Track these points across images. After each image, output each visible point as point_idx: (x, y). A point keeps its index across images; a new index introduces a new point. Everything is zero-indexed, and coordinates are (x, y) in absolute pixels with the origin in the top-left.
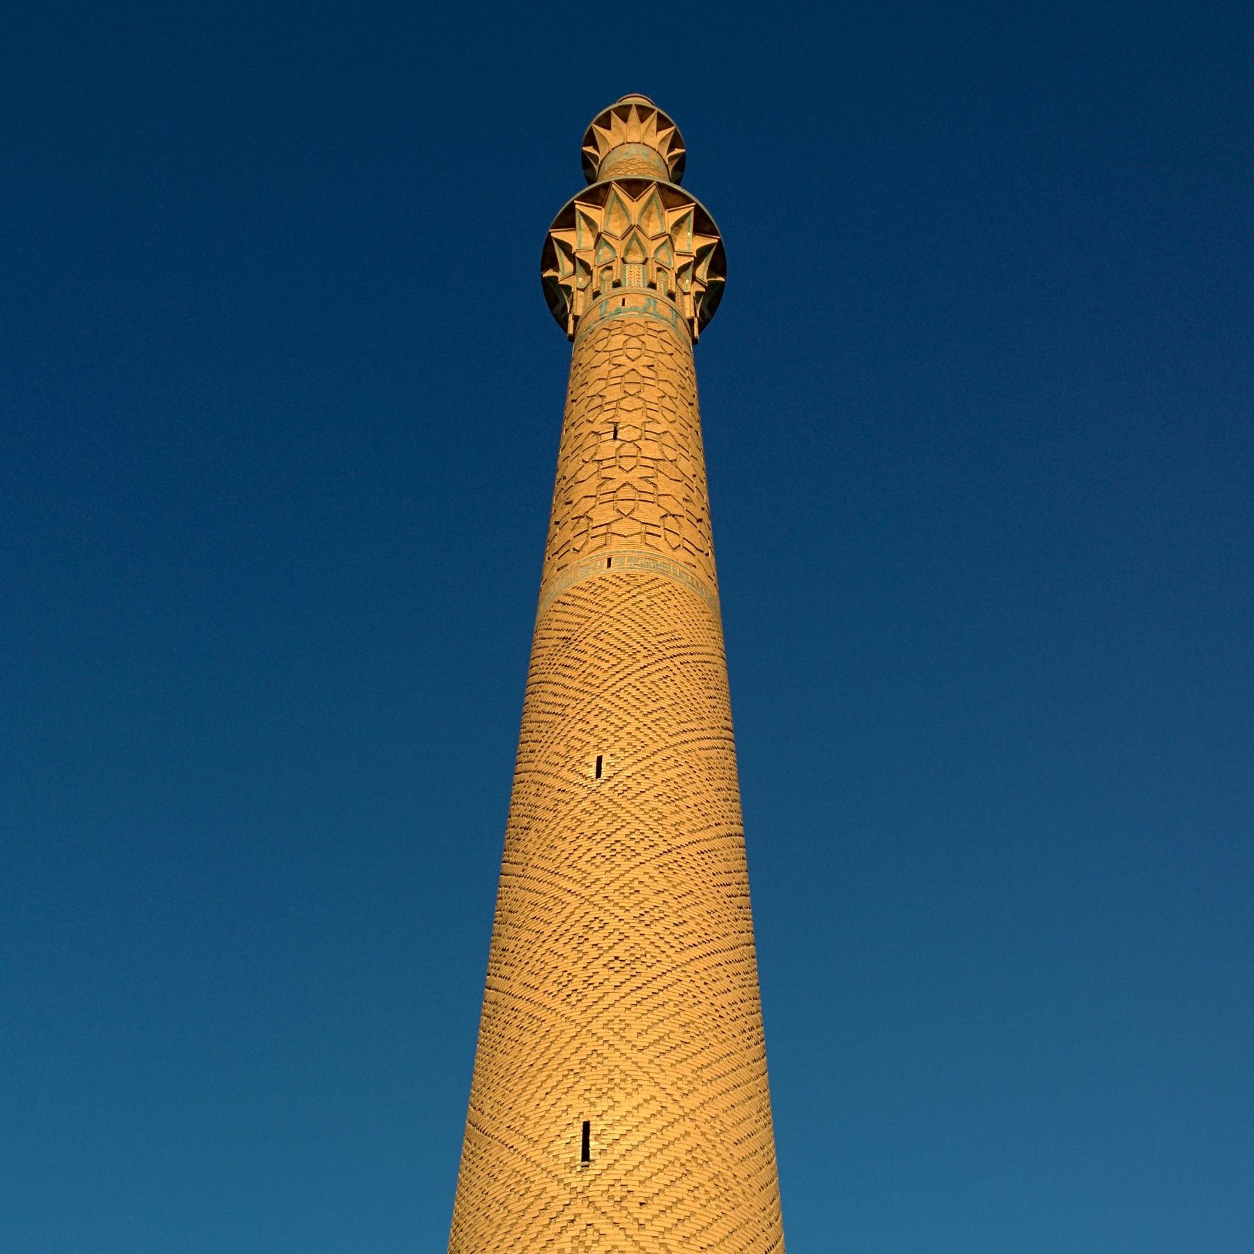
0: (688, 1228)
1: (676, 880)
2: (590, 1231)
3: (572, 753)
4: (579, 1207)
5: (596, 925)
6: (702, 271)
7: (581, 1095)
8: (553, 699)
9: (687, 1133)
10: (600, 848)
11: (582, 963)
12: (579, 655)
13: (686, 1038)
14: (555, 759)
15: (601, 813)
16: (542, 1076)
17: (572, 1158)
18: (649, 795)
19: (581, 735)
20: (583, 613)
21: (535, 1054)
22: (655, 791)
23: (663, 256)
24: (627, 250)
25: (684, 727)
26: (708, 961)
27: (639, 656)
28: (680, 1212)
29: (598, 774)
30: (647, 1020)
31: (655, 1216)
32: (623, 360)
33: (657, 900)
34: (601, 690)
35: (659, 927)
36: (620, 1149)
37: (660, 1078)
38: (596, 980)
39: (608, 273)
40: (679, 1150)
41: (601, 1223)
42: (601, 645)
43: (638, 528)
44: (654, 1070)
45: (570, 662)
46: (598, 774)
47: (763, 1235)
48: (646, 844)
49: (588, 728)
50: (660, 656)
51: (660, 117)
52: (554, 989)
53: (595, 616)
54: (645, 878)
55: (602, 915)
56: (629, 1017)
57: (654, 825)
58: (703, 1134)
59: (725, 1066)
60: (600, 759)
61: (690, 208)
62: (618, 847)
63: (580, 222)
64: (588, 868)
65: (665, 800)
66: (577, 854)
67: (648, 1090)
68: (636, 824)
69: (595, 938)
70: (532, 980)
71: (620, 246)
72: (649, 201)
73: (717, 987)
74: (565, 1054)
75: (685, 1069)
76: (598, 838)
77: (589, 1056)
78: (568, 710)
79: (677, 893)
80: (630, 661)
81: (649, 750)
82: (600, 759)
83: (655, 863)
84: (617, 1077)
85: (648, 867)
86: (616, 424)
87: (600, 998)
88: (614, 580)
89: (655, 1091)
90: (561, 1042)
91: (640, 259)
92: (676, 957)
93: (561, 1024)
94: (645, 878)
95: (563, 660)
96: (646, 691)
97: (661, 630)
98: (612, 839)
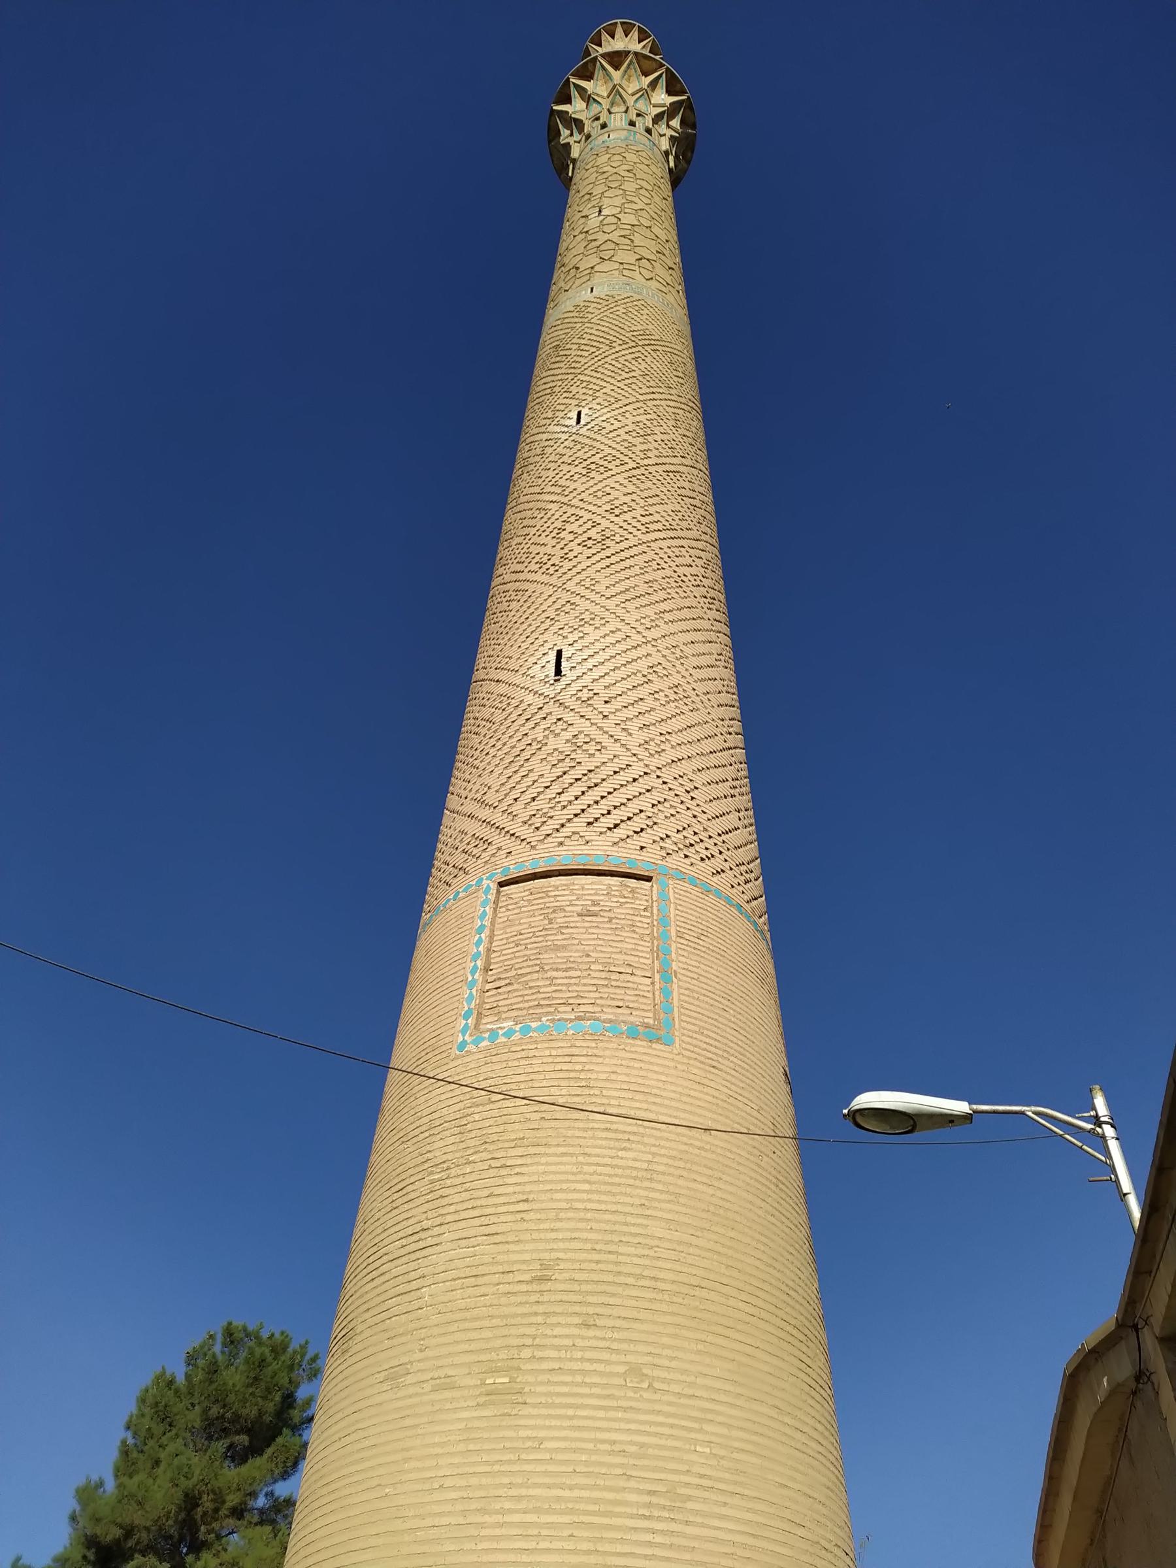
0: (648, 719)
1: (643, 487)
2: (560, 723)
5: (573, 519)
6: (676, 123)
10: (579, 469)
11: (559, 546)
13: (650, 591)
14: (544, 422)
15: (579, 446)
17: (547, 676)
18: (621, 432)
19: (565, 401)
22: (627, 429)
23: (642, 105)
24: (612, 104)
25: (652, 390)
28: (641, 707)
29: (578, 422)
30: (614, 578)
32: (608, 168)
33: (628, 499)
35: (628, 516)
37: (626, 617)
38: (571, 555)
40: (642, 665)
41: (569, 717)
43: (617, 266)
46: (578, 422)
47: (730, 783)
48: (618, 462)
51: (640, 30)
54: (617, 486)
55: (577, 512)
56: (598, 576)
57: (625, 451)
58: (664, 656)
59: (686, 613)
60: (579, 413)
61: (663, 70)
62: (593, 466)
65: (634, 434)
67: (614, 624)
68: (608, 451)
69: (569, 528)
70: (519, 567)
71: (606, 103)
72: (629, 65)
73: (679, 561)
74: (543, 607)
75: (649, 611)
81: (620, 404)
82: (579, 413)
83: (626, 475)
84: (587, 616)
85: (619, 478)
89: (620, 625)
90: (540, 600)
94: (617, 486)
97: (634, 328)
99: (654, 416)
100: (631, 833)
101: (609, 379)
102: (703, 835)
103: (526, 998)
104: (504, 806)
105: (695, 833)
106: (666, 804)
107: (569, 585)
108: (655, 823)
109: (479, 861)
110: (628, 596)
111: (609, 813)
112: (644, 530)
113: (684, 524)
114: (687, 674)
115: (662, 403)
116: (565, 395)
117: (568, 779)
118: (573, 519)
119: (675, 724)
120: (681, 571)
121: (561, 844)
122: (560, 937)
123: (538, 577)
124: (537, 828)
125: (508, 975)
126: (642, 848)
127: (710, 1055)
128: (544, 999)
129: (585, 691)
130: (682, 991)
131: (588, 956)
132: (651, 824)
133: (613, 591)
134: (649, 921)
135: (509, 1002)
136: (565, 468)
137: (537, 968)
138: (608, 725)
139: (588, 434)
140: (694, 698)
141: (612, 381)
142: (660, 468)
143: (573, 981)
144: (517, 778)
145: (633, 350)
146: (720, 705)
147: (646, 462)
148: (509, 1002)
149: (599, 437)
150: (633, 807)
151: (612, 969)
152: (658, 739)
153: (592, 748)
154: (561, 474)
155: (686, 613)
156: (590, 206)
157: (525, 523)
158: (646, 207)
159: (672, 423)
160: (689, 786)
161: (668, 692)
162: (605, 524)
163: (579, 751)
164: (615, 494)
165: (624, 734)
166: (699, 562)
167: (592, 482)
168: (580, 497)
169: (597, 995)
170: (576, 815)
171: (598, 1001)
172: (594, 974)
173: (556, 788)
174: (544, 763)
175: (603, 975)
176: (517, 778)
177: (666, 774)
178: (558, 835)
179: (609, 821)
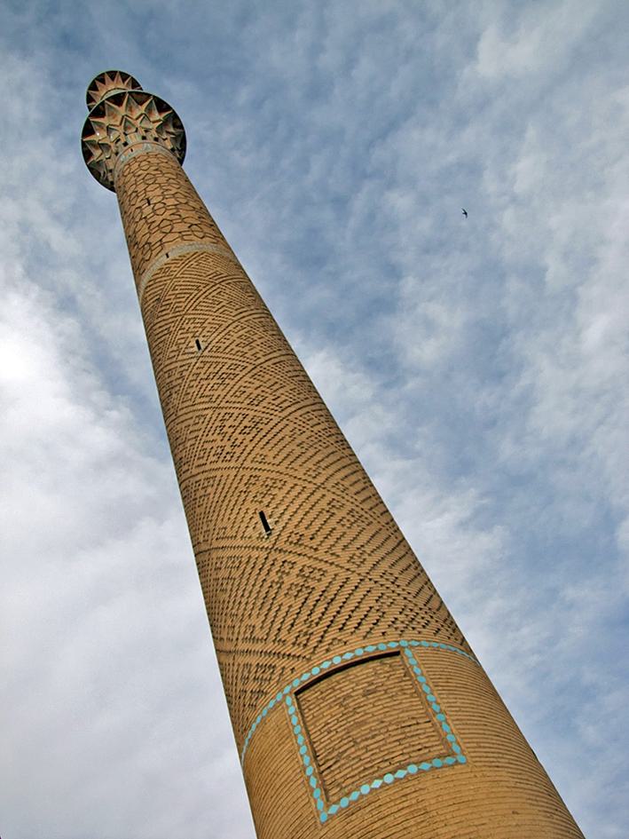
0: (344, 541)
1: (265, 380)
2: (286, 564)
3: (181, 346)
4: (274, 555)
7: (252, 501)
8: (161, 329)
9: (324, 495)
11: (226, 439)
12: (167, 302)
13: (304, 450)
14: (172, 354)
15: (208, 365)
16: (226, 502)
17: (260, 534)
18: (233, 346)
19: (182, 336)
21: (217, 495)
22: (235, 343)
23: (146, 125)
24: (125, 128)
26: (300, 412)
28: (337, 534)
29: (199, 348)
30: (276, 450)
31: (322, 542)
33: (259, 391)
35: (264, 404)
36: (286, 517)
37: (296, 474)
38: (238, 443)
39: (119, 143)
41: (291, 558)
42: (177, 292)
43: (177, 235)
44: (291, 472)
45: (163, 308)
46: (199, 348)
48: (240, 368)
49: (185, 331)
52: (215, 458)
55: (228, 411)
59: (332, 458)
60: (197, 342)
62: (224, 376)
63: (95, 127)
64: (211, 393)
66: (202, 390)
68: (230, 362)
69: (228, 424)
70: (201, 461)
71: (121, 129)
74: (234, 485)
75: (309, 465)
76: (211, 376)
77: (249, 480)
78: (171, 329)
79: (268, 384)
80: (196, 292)
81: (223, 327)
82: (197, 342)
83: (250, 375)
84: (269, 482)
85: (246, 379)
86: (147, 199)
87: (244, 450)
89: (296, 481)
90: (230, 481)
91: (135, 130)
92: (280, 414)
93: (225, 473)
98: (220, 373)
99: (250, 329)
100: (372, 626)
101: (207, 313)
102: (416, 610)
103: (354, 767)
104: (272, 637)
105: (411, 610)
106: (384, 597)
107: (245, 465)
108: (384, 613)
109: (272, 683)
110: (291, 459)
111: (350, 616)
112: (280, 410)
113: (302, 396)
114: (353, 501)
115: (250, 317)
116: (180, 332)
117: (310, 603)
118: (227, 417)
119: (364, 538)
120: (315, 429)
121: (328, 650)
122: (357, 716)
123: (219, 465)
124: (305, 645)
125: (334, 755)
126: (383, 633)
127: (492, 759)
128: (367, 763)
129: (293, 535)
130: (455, 722)
131: (382, 722)
132: (381, 614)
133: (279, 459)
134: (410, 683)
135: (342, 774)
136: (205, 382)
137: (352, 744)
138: (320, 554)
139: (210, 354)
140: (366, 515)
141: (211, 313)
142: (270, 363)
143: (381, 743)
144: (272, 613)
145: (214, 288)
146: (382, 514)
147: (259, 362)
148: (342, 774)
149: (219, 355)
150: (365, 607)
151: (403, 725)
152: (358, 553)
153: (317, 575)
154: (204, 387)
155: (332, 458)
157: (191, 429)
158: (179, 190)
159: (261, 329)
160: (392, 579)
161: (349, 517)
162: (252, 413)
163: (310, 580)
164: (248, 391)
165: (334, 557)
166: (323, 419)
167: (228, 388)
168: (225, 400)
169: (401, 747)
170: (328, 626)
171: (405, 751)
172: (393, 733)
173: (305, 612)
174: (288, 597)
175: (399, 731)
176: (272, 613)
177: (375, 575)
178: (322, 644)
179: (353, 623)
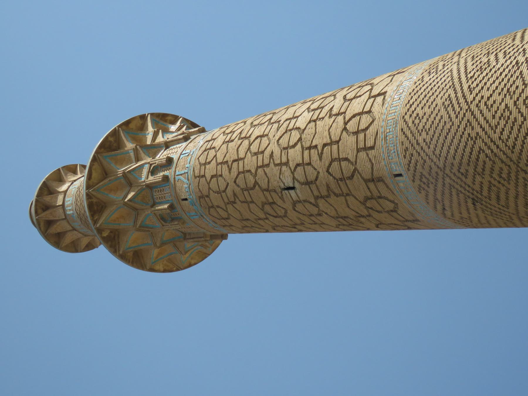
12: (485, 189)
20: (447, 191)
27: (473, 135)
34: (511, 164)
42: (471, 171)
45: (493, 196)
50: (468, 114)
53: (448, 180)
88: (412, 169)
95: (494, 202)
96: (503, 122)
97: (446, 117)
156: (279, 202)
